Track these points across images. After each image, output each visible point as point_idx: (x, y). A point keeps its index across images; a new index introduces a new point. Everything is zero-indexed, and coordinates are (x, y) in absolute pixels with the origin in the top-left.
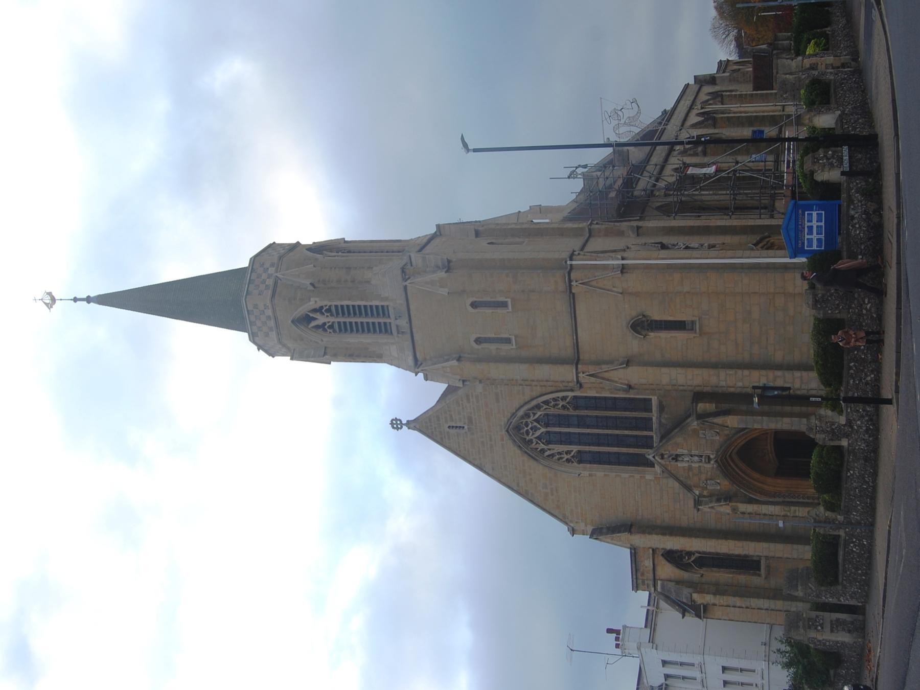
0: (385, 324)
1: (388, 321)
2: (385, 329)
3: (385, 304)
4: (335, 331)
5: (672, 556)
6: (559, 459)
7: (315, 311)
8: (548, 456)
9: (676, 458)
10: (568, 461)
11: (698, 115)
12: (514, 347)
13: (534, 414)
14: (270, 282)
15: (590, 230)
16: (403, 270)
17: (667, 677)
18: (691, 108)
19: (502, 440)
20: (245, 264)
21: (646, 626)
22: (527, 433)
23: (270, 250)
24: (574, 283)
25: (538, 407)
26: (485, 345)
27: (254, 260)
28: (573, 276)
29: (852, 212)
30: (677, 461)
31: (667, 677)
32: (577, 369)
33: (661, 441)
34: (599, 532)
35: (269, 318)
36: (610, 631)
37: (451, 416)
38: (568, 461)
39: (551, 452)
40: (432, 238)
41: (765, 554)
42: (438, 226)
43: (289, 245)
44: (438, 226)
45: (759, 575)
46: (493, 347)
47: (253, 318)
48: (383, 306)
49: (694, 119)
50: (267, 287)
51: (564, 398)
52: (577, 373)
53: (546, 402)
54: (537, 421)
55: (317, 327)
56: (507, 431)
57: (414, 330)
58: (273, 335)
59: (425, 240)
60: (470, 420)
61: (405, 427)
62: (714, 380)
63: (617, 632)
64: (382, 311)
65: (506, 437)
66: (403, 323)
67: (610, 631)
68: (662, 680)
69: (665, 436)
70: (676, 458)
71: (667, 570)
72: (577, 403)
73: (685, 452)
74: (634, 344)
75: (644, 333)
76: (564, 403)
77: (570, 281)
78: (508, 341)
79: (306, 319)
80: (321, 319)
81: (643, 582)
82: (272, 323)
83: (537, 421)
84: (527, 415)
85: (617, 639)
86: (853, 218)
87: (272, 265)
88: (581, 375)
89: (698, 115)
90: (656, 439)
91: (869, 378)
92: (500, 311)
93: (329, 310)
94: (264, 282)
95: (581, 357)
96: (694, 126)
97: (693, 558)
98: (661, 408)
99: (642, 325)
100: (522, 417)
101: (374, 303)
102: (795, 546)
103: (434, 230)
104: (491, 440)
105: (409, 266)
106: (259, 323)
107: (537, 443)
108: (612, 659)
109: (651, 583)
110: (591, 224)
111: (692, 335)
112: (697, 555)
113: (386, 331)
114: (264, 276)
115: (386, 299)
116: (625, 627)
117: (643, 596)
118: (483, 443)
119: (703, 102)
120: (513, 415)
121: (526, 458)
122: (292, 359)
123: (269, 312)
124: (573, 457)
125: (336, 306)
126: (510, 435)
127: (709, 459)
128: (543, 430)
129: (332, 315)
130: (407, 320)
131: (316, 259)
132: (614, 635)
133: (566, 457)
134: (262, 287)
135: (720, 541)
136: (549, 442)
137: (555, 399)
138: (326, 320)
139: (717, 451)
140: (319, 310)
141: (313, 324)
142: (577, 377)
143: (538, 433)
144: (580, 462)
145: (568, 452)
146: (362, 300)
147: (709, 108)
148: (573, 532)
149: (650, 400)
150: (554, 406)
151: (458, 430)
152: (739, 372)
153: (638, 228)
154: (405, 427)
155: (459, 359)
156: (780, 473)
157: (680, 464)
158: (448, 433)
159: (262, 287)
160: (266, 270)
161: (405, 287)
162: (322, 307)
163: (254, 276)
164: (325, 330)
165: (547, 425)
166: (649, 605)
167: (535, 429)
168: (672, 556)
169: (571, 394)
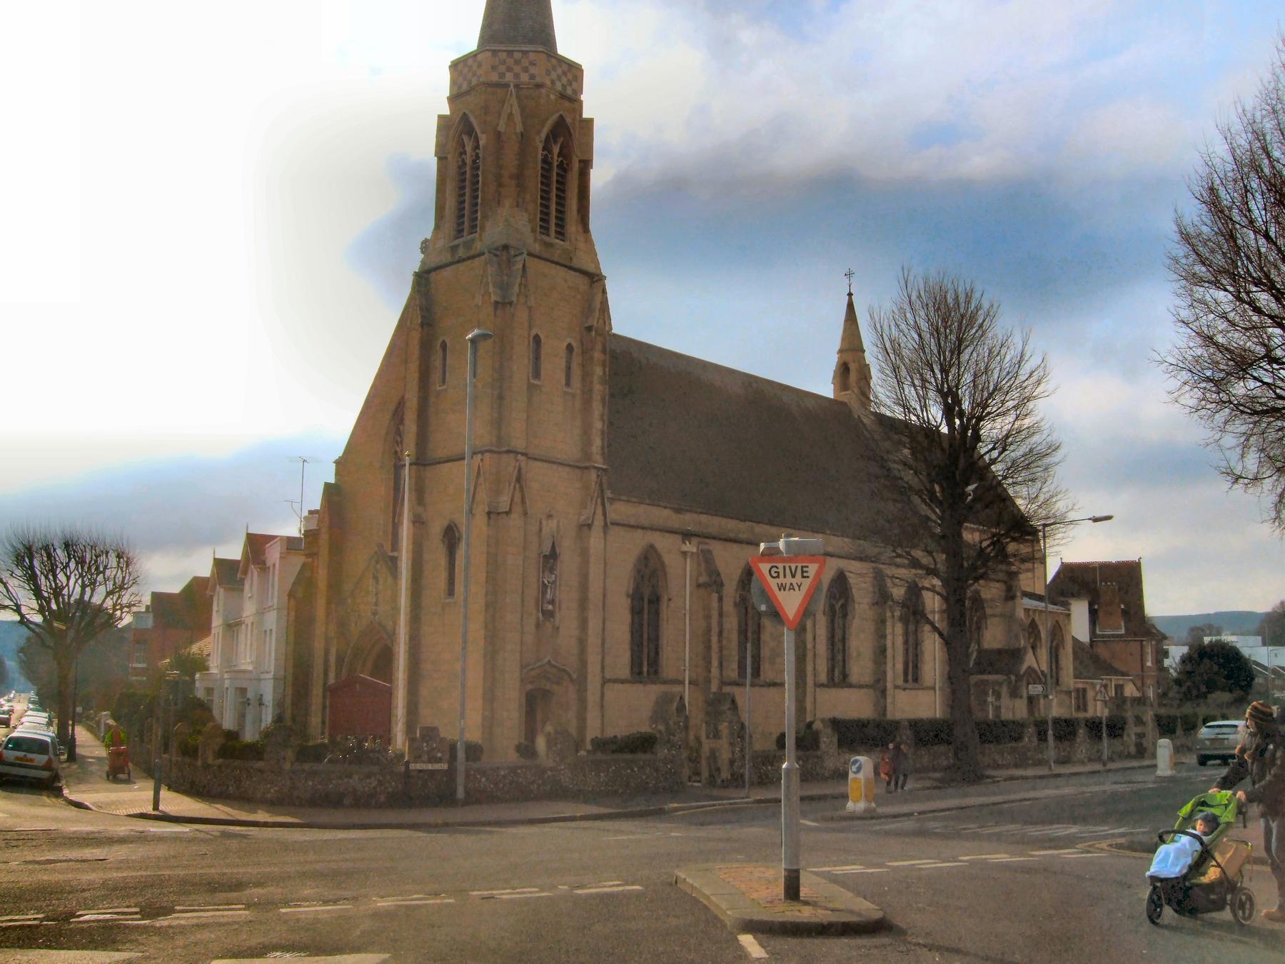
1: (465, 233)
2: (460, 232)
4: (460, 167)
7: (477, 140)
9: (376, 578)
14: (509, 77)
15: (587, 468)
16: (506, 247)
24: (479, 456)
26: (440, 353)
28: (487, 455)
29: (356, 777)
34: (329, 489)
50: (502, 75)
55: (464, 147)
57: (454, 267)
66: (461, 253)
70: (376, 578)
73: (380, 587)
74: (436, 529)
77: (482, 453)
78: (444, 382)
79: (470, 131)
86: (350, 776)
87: (532, 77)
93: (477, 156)
94: (509, 69)
95: (428, 468)
99: (451, 537)
105: (512, 252)
108: (297, 506)
110: (598, 469)
114: (517, 69)
115: (483, 228)
122: (440, 117)
123: (474, 81)
127: (375, 614)
134: (502, 68)
139: (380, 624)
141: (465, 138)
148: (338, 463)
153: (589, 526)
155: (422, 325)
159: (502, 68)
160: (526, 70)
162: (477, 147)
164: (461, 154)
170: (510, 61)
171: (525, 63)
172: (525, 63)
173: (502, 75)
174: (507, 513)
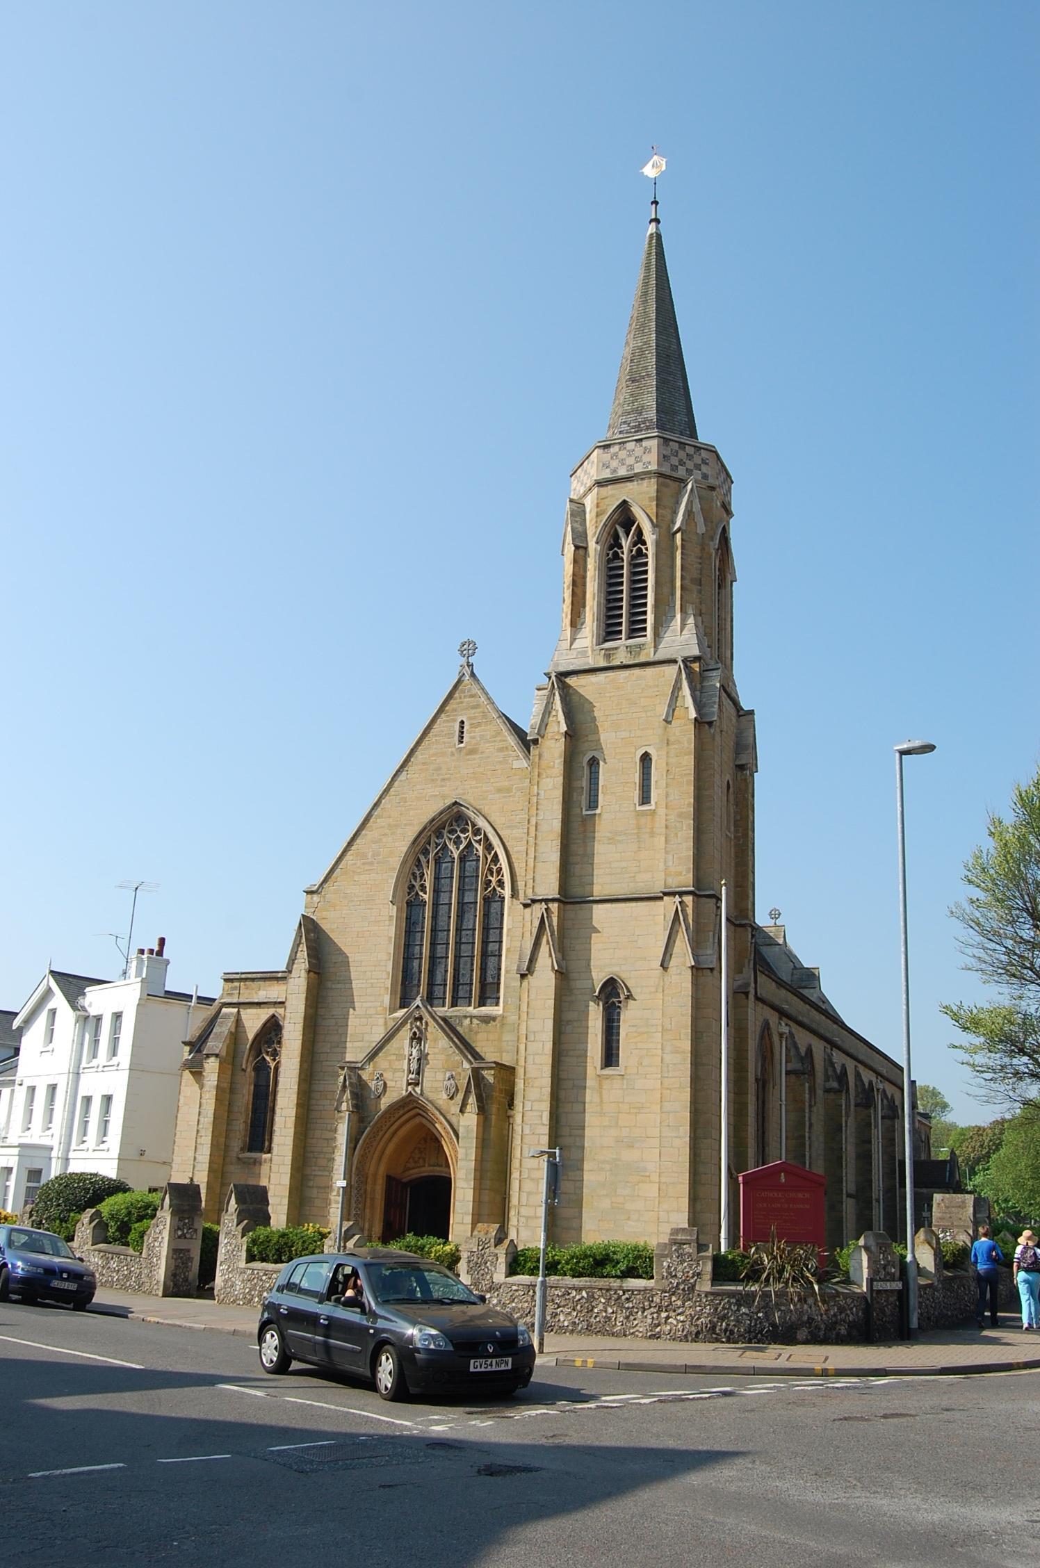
0: (620, 632)
1: (623, 636)
3: (649, 632)
4: (609, 561)
5: (272, 1030)
6: (414, 874)
7: (640, 533)
8: (419, 860)
10: (412, 887)
11: (871, 1083)
12: (584, 813)
13: (479, 842)
14: (681, 473)
17: (99, 1019)
18: (878, 1074)
19: (444, 797)
20: (704, 437)
21: (167, 992)
22: (452, 832)
23: (723, 475)
25: (489, 847)
26: (586, 771)
27: (712, 451)
30: (412, 1039)
31: (99, 1019)
32: (553, 900)
33: (444, 1019)
35: (631, 467)
36: (162, 942)
37: (479, 725)
38: (412, 887)
39: (424, 865)
40: (736, 703)
41: (275, 1158)
42: (751, 713)
43: (730, 503)
44: (751, 713)
45: (242, 1149)
46: (584, 783)
47: (631, 446)
48: (645, 629)
49: (867, 1076)
50: (674, 468)
51: (501, 883)
52: (547, 901)
53: (496, 859)
54: (470, 845)
55: (616, 537)
56: (456, 803)
58: (607, 474)
59: (734, 695)
60: (472, 752)
61: (463, 661)
62: (533, 1094)
63: (160, 953)
64: (636, 629)
65: (449, 802)
66: (621, 657)
67: (162, 942)
68: (93, 1012)
69: (449, 1027)
71: (253, 1021)
72: (492, 901)
75: (603, 996)
76: (493, 884)
80: (626, 543)
81: (235, 988)
82: (622, 472)
83: (470, 845)
84: (477, 832)
85: (151, 951)
88: (544, 905)
89: (871, 1083)
90: (441, 1011)
91: (562, 1318)
92: (636, 794)
93: (640, 554)
94: (682, 463)
95: (569, 907)
96: (858, 1075)
97: (268, 1058)
98: (487, 1020)
100: (474, 825)
101: (650, 617)
102: (286, 1201)
103: (746, 706)
104: (443, 780)
106: (623, 454)
107: (437, 845)
108: (123, 944)
109: (235, 1000)
111: (599, 1067)
112: (272, 1065)
113: (609, 633)
114: (690, 465)
116: (168, 962)
117: (215, 989)
118: (439, 769)
119: (884, 1091)
120: (479, 812)
121: (418, 828)
124: (417, 894)
125: (646, 564)
126: (449, 807)
128: (456, 855)
129: (633, 558)
130: (627, 662)
131: (712, 539)
132: (156, 948)
133: (417, 885)
134: (675, 461)
135: (295, 1097)
136: (438, 862)
137: (499, 870)
138: (625, 550)
140: (640, 539)
142: (540, 901)
143: (451, 847)
144: (409, 904)
145: (423, 888)
146: (656, 600)
147: (878, 1098)
149: (497, 1004)
150: (490, 870)
151: (457, 734)
152: (546, 1130)
153: (747, 994)
154: (463, 661)
156: (392, 1183)
157: (407, 1042)
158: (455, 720)
159: (675, 461)
160: (698, 467)
161: (675, 661)
163: (690, 450)
164: (611, 548)
165: (463, 859)
166: (199, 998)
167: (457, 842)
168: (272, 1030)
169: (507, 892)
170: (682, 454)
171: (697, 460)
172: (697, 460)
173: (674, 468)
174: (712, 969)
